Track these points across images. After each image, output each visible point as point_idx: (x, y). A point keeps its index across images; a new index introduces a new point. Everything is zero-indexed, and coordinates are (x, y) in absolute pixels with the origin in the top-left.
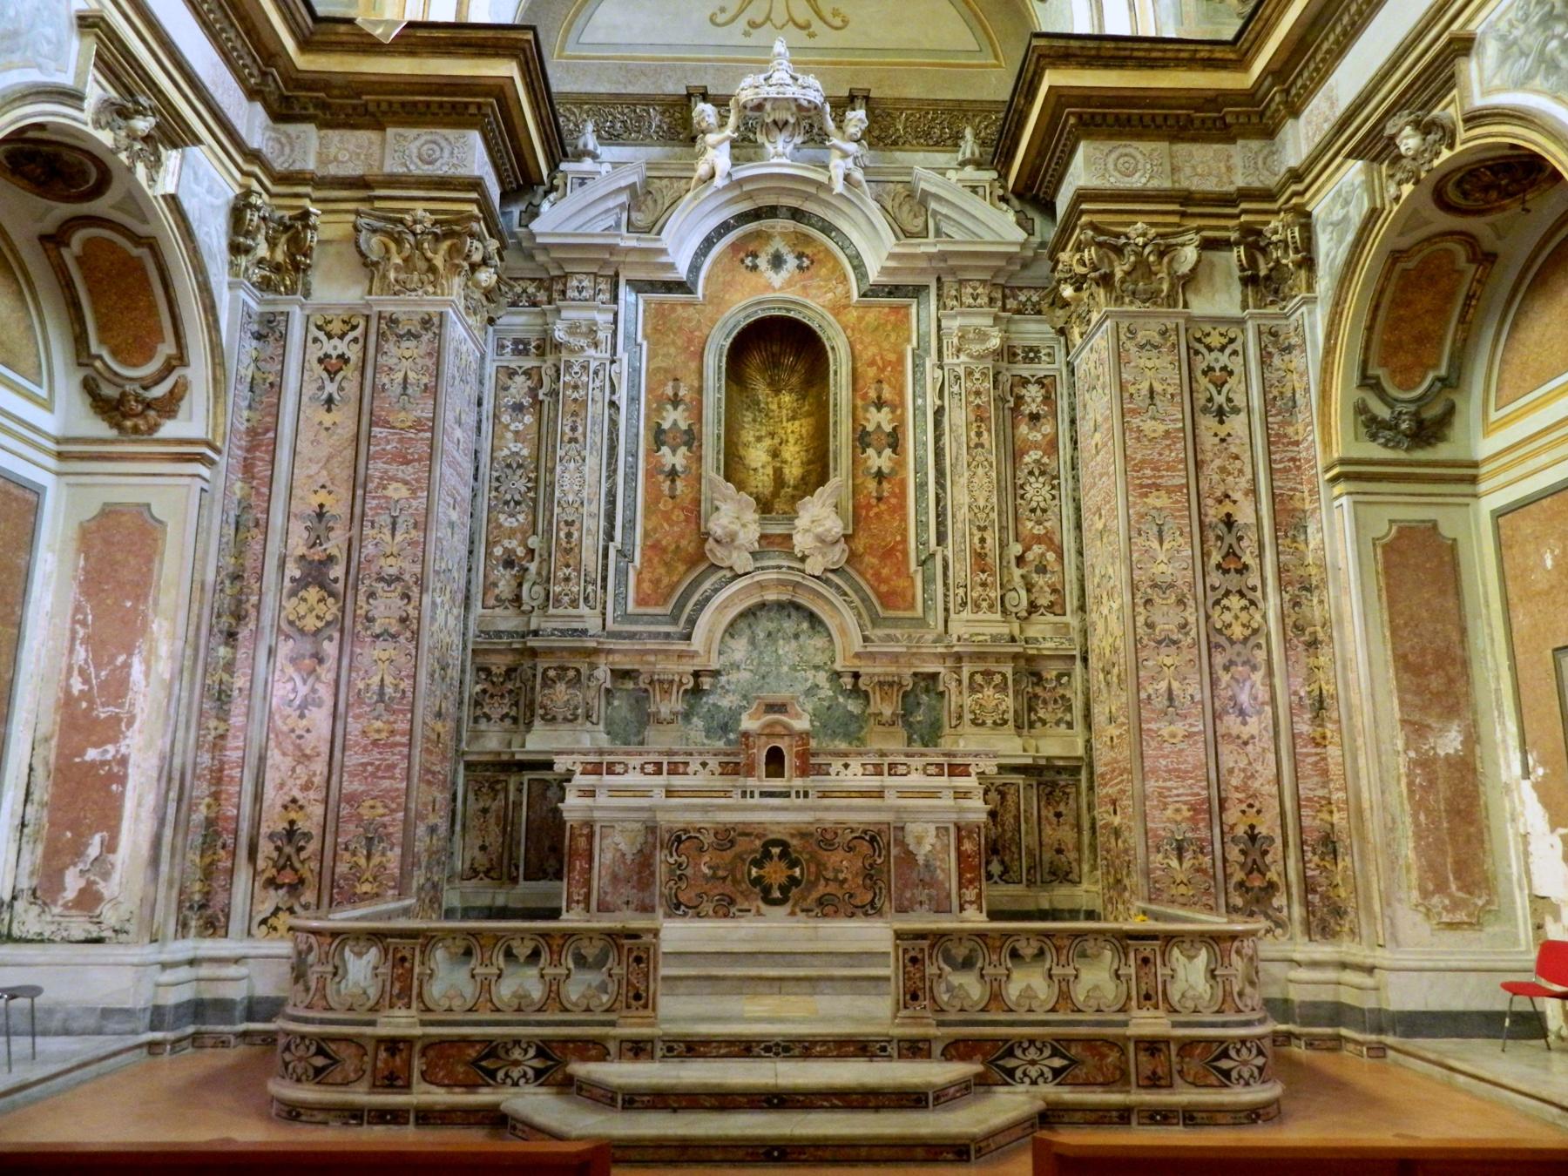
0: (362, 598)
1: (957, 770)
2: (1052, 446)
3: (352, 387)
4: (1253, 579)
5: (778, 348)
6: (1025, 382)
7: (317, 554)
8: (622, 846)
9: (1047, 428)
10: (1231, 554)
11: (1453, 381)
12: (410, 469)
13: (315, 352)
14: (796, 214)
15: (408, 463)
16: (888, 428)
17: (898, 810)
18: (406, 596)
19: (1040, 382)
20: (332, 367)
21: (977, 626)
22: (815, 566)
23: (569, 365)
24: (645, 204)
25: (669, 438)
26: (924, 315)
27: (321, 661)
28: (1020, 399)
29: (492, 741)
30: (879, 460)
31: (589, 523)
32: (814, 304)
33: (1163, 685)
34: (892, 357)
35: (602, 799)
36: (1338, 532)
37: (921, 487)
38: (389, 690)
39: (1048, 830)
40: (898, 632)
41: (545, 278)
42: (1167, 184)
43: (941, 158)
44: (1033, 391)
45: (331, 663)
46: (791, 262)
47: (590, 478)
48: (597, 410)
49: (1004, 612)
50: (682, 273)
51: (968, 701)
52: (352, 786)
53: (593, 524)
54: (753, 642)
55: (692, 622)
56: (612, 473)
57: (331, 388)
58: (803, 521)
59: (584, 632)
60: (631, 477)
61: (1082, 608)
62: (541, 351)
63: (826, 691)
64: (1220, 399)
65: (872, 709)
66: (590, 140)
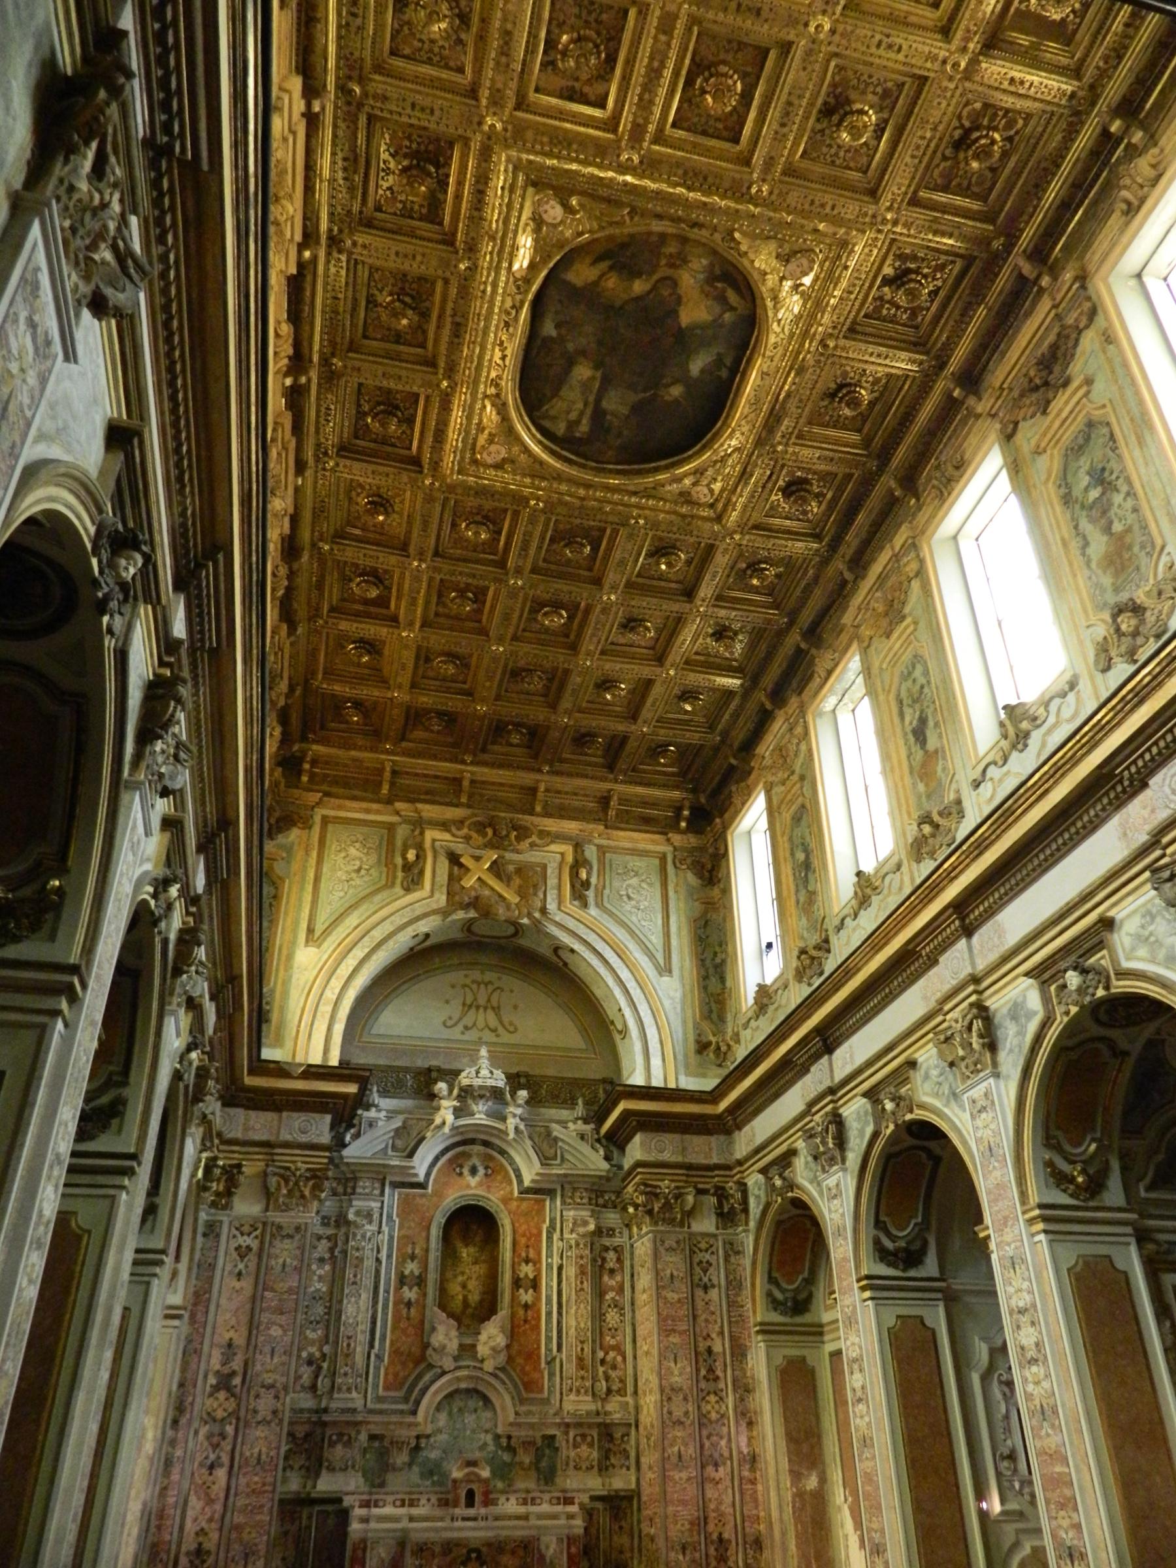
0: (252, 1398)
1: (569, 1501)
2: (621, 1290)
3: (252, 1266)
4: (722, 1385)
5: (473, 1223)
6: (607, 1249)
7: (226, 1370)
8: (383, 1555)
9: (618, 1278)
10: (711, 1370)
11: (811, 1281)
12: (284, 1318)
13: (233, 1244)
14: (486, 1144)
15: (282, 1313)
16: (531, 1276)
17: (539, 1528)
18: (277, 1397)
19: (615, 1249)
20: (243, 1252)
21: (578, 1404)
22: (489, 1366)
23: (355, 1235)
24: (408, 1141)
25: (407, 1281)
26: (553, 1208)
27: (224, 1439)
28: (604, 1259)
29: (294, 1484)
30: (526, 1296)
31: (360, 1337)
32: (493, 1200)
33: (676, 1449)
34: (535, 1231)
35: (373, 1525)
36: (760, 1362)
37: (549, 1314)
38: (264, 1457)
39: (615, 1538)
40: (533, 1408)
41: (348, 1181)
42: (680, 1159)
43: (564, 1114)
44: (611, 1255)
45: (230, 1440)
46: (481, 1171)
47: (363, 1308)
48: (369, 1263)
49: (594, 1395)
50: (421, 1178)
51: (572, 1454)
52: (239, 1519)
53: (362, 1338)
54: (450, 1414)
55: (418, 1403)
56: (375, 1303)
57: (241, 1266)
58: (483, 1337)
59: (354, 1410)
60: (386, 1306)
61: (636, 1392)
62: (338, 1225)
63: (491, 1448)
64: (705, 1279)
65: (517, 1459)
66: (376, 1098)
